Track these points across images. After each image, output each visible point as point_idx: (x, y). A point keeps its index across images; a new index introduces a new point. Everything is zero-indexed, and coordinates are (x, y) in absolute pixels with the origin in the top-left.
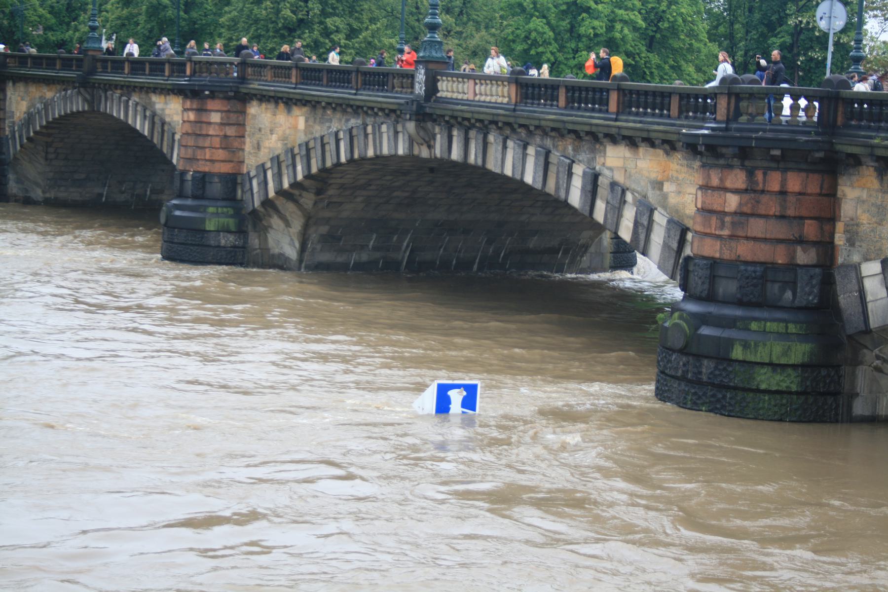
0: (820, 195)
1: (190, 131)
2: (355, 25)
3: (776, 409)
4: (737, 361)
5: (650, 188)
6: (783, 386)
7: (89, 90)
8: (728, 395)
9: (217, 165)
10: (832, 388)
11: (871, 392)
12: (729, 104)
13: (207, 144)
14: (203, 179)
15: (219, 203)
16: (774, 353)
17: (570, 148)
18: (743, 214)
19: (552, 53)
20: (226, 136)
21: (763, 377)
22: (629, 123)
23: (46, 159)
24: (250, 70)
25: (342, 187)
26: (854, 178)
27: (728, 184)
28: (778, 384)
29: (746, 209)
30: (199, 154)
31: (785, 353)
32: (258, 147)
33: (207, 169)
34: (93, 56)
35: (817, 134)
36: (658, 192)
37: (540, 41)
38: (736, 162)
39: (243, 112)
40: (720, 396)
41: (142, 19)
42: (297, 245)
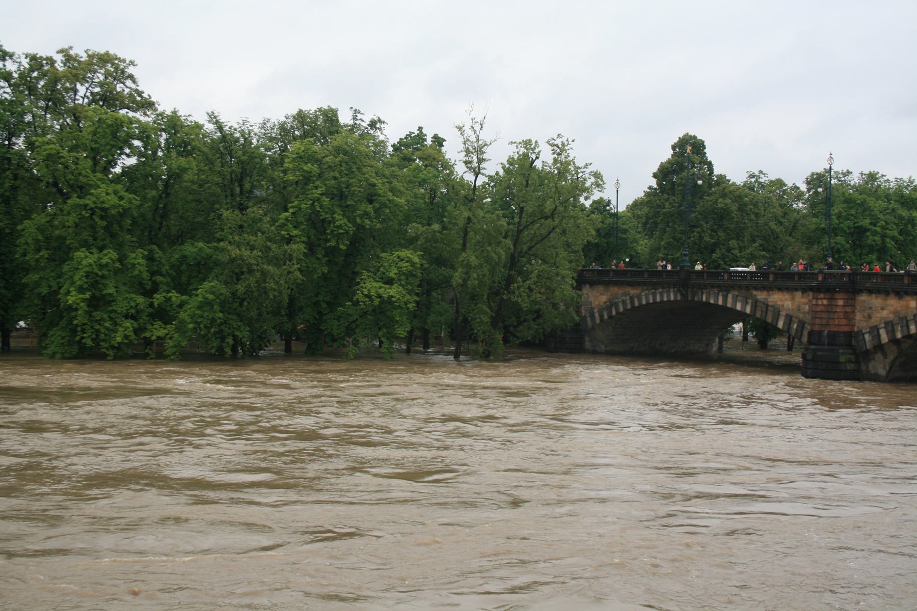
1: (824, 309)
2: (741, 244)
9: (842, 327)
13: (836, 316)
14: (833, 336)
19: (850, 257)
20: (846, 312)
30: (831, 322)
32: (870, 317)
33: (836, 330)
37: (842, 250)
39: (854, 299)
42: (888, 368)
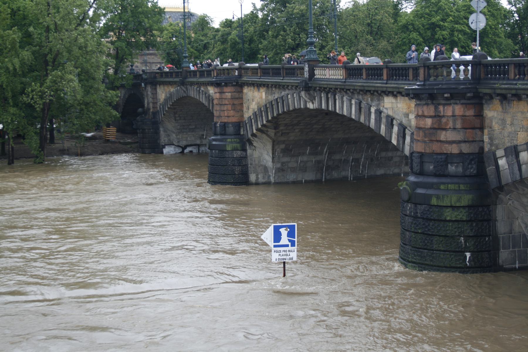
0: (474, 116)
3: (456, 230)
4: (434, 206)
5: (403, 117)
6: (459, 218)
7: (185, 86)
8: (431, 224)
10: (486, 218)
11: (509, 218)
12: (424, 72)
14: (224, 125)
15: (233, 137)
16: (452, 201)
17: (369, 99)
18: (434, 128)
20: (233, 104)
21: (448, 214)
22: (392, 85)
23: (175, 120)
24: (243, 71)
25: (286, 125)
26: (491, 106)
27: (426, 114)
28: (456, 217)
29: (436, 126)
31: (459, 200)
33: (226, 121)
34: (186, 70)
35: (470, 84)
36: (407, 119)
38: (429, 102)
40: (427, 224)
41: (228, 50)
42: (271, 155)
